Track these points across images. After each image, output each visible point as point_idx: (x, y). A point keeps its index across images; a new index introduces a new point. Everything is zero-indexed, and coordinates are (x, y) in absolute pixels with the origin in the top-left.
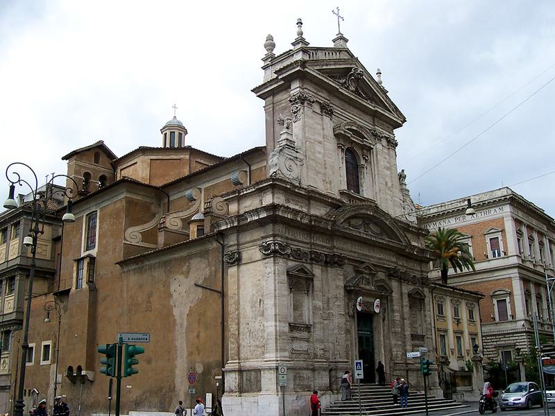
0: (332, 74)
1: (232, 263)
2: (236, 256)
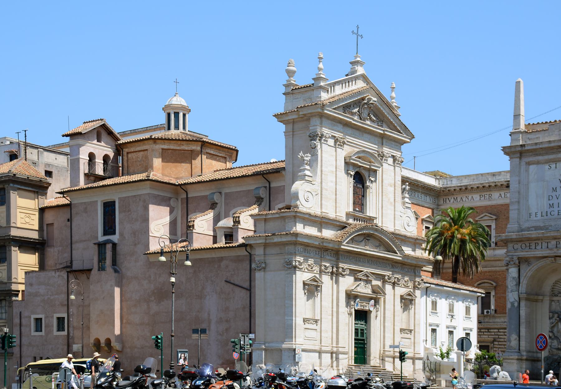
0: (347, 108)
1: (260, 270)
2: (263, 265)
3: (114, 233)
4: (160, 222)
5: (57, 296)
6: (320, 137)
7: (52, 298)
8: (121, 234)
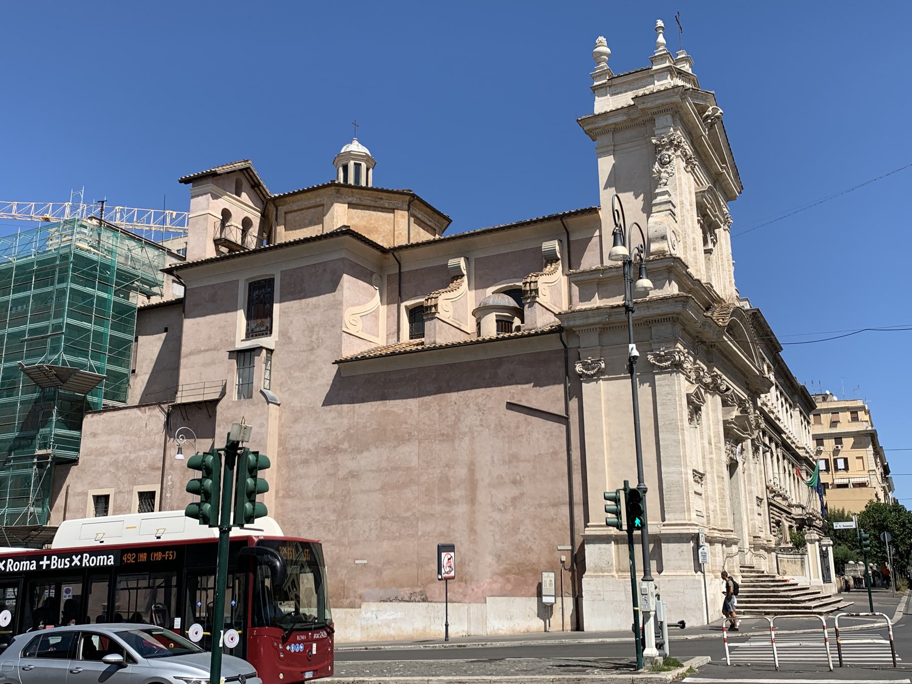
3: (268, 331)
4: (357, 309)
5: (143, 453)
6: (676, 145)
7: (133, 456)
8: (283, 334)
